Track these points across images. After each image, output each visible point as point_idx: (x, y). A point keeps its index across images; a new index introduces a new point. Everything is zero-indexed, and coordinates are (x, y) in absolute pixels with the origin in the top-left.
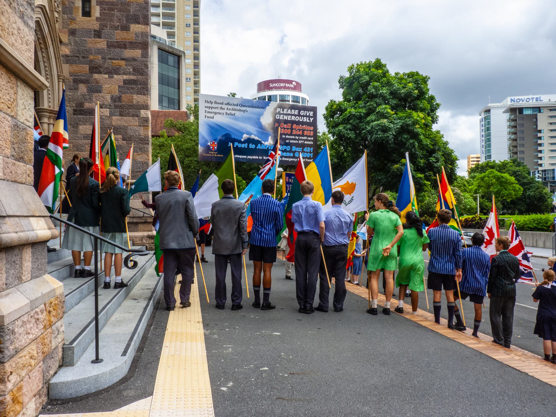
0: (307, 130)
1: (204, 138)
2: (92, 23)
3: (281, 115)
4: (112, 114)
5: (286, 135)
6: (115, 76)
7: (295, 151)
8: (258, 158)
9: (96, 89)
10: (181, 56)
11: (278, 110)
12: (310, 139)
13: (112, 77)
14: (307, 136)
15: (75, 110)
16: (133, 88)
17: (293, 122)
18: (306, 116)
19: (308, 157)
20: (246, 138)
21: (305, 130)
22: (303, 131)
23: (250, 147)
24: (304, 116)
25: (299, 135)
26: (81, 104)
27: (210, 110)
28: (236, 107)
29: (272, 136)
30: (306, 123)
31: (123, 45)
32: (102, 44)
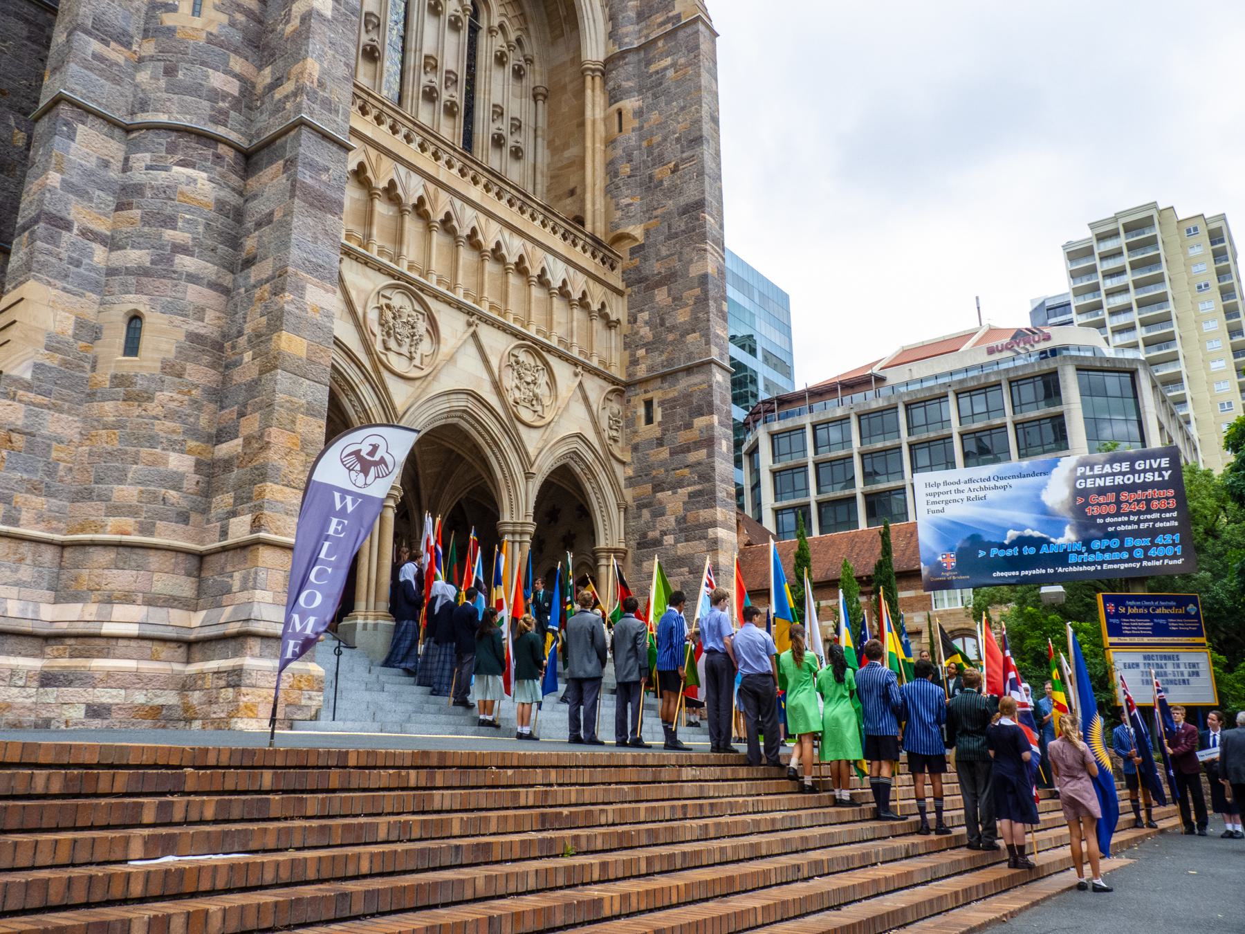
0: (1159, 499)
1: (929, 549)
2: (654, 431)
3: (1088, 480)
4: (677, 541)
5: (1104, 517)
6: (679, 490)
7: (1135, 547)
8: (1044, 571)
9: (659, 513)
10: (1137, 370)
11: (1080, 471)
12: (1168, 515)
13: (676, 493)
14: (1160, 511)
15: (638, 544)
16: (699, 502)
17: (1118, 489)
18: (1152, 470)
19: (1170, 554)
20: (1014, 538)
21: (1153, 499)
22: (1148, 501)
23: (1025, 553)
24: (1145, 471)
25: (1139, 513)
26: (644, 535)
27: (937, 499)
28: (987, 484)
29: (1072, 525)
30: (1153, 485)
31: (686, 449)
32: (664, 453)
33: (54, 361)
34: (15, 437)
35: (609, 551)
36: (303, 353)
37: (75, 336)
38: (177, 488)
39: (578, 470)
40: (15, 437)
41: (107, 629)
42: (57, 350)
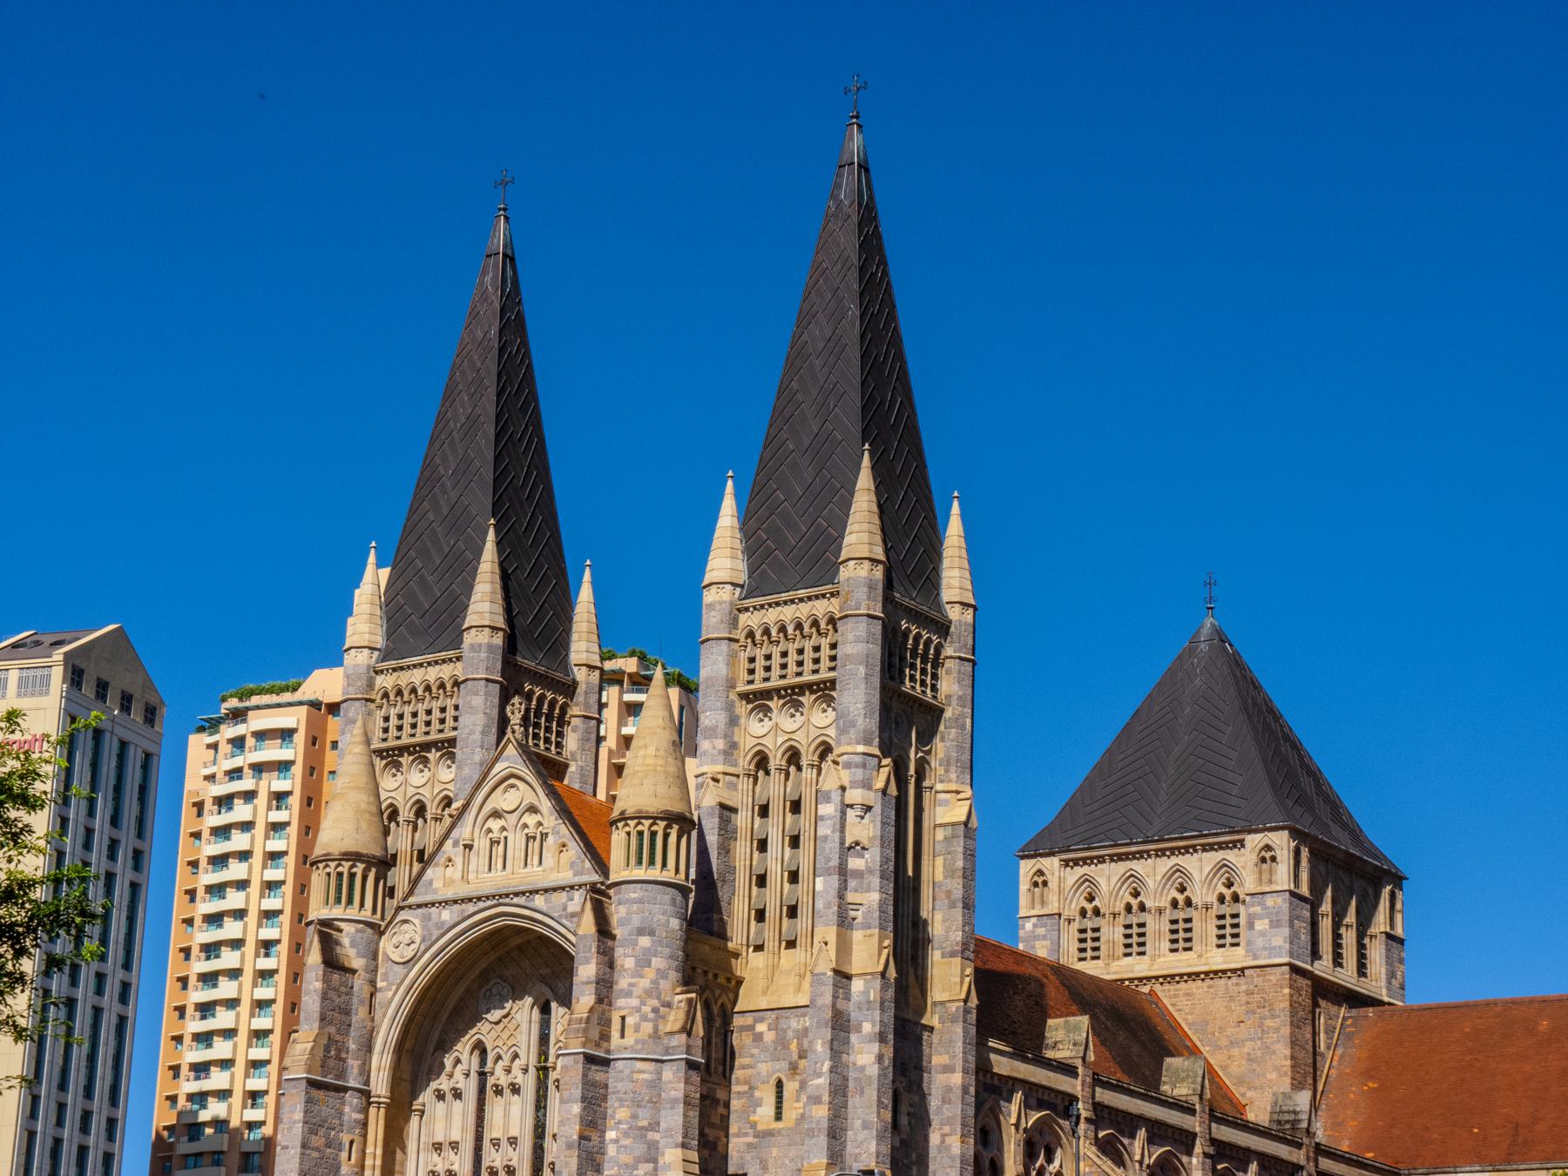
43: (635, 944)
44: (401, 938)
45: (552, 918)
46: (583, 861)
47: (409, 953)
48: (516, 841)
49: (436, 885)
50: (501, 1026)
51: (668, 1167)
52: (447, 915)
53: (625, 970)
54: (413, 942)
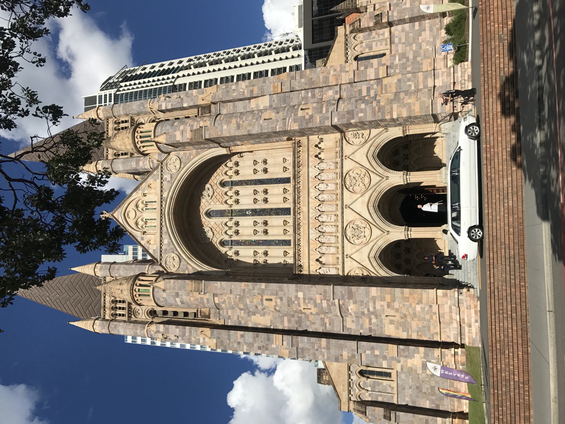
33: (401, 328)
34: (419, 334)
35: (404, 133)
36: (389, 296)
37: (394, 324)
38: (424, 308)
39: (378, 151)
40: (419, 334)
41: (458, 320)
42: (398, 328)
43: (176, 126)
44: (171, 264)
45: (171, 186)
46: (154, 175)
47: (177, 259)
48: (146, 215)
49: (155, 248)
50: (215, 232)
51: (257, 105)
52: (166, 241)
53: (184, 128)
54: (173, 257)
